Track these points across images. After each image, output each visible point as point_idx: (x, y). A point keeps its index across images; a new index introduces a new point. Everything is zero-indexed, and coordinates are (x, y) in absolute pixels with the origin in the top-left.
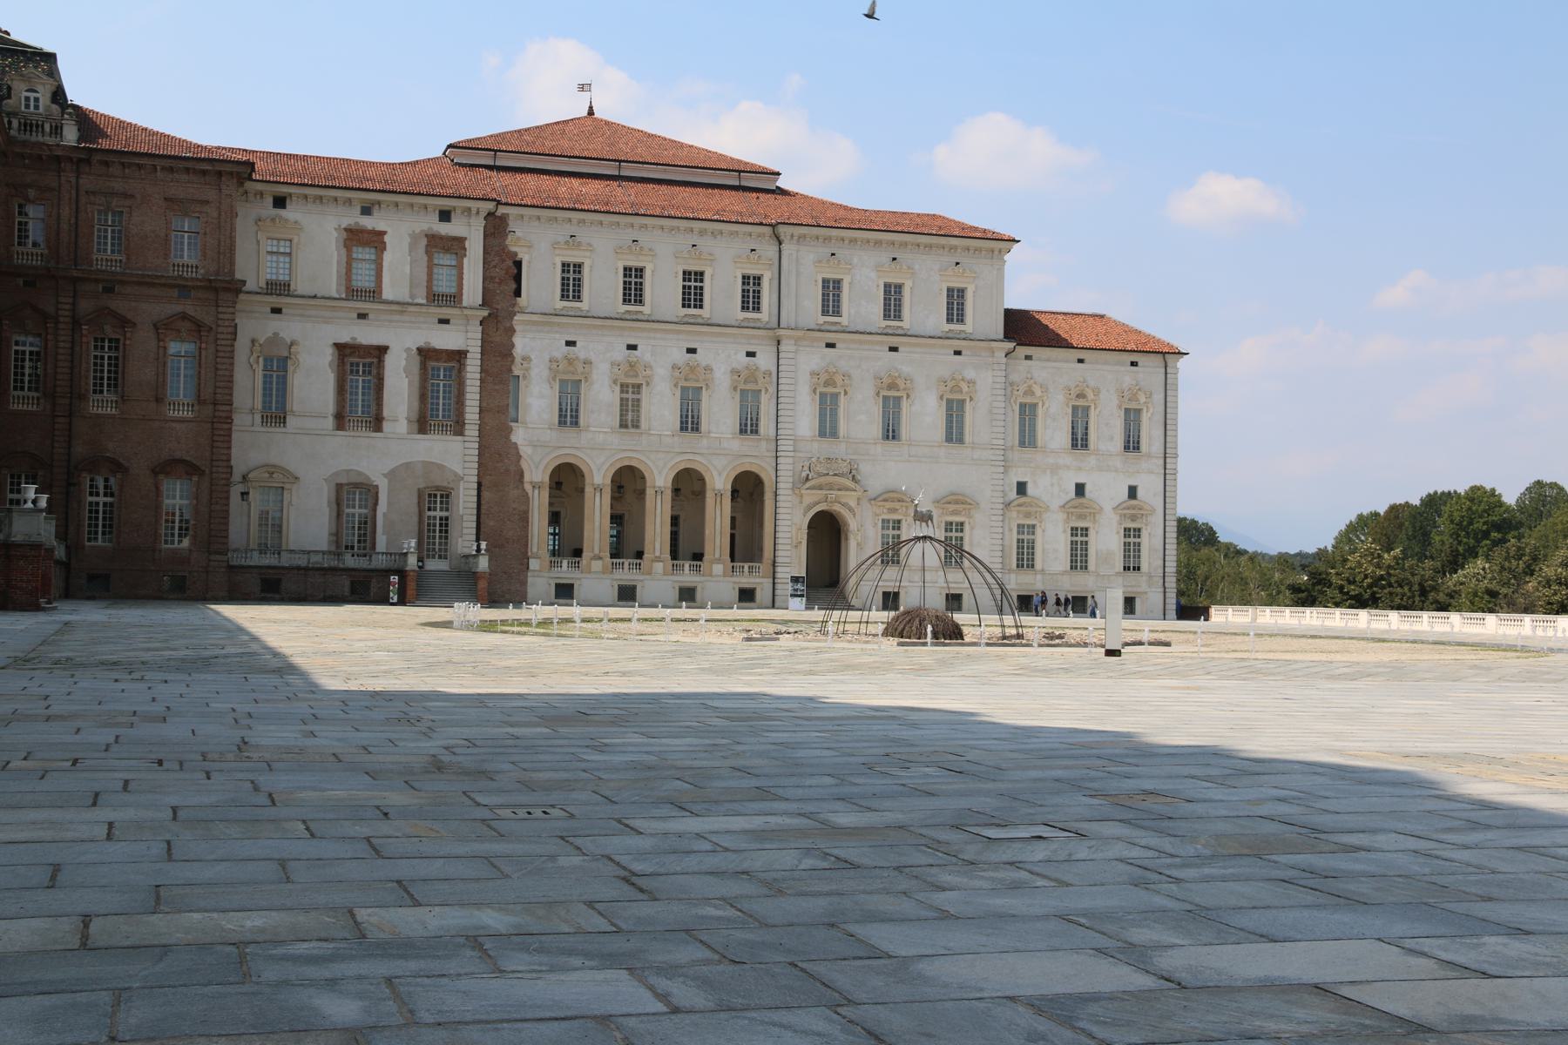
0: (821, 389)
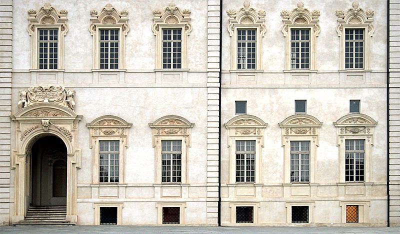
0: (101, 25)
